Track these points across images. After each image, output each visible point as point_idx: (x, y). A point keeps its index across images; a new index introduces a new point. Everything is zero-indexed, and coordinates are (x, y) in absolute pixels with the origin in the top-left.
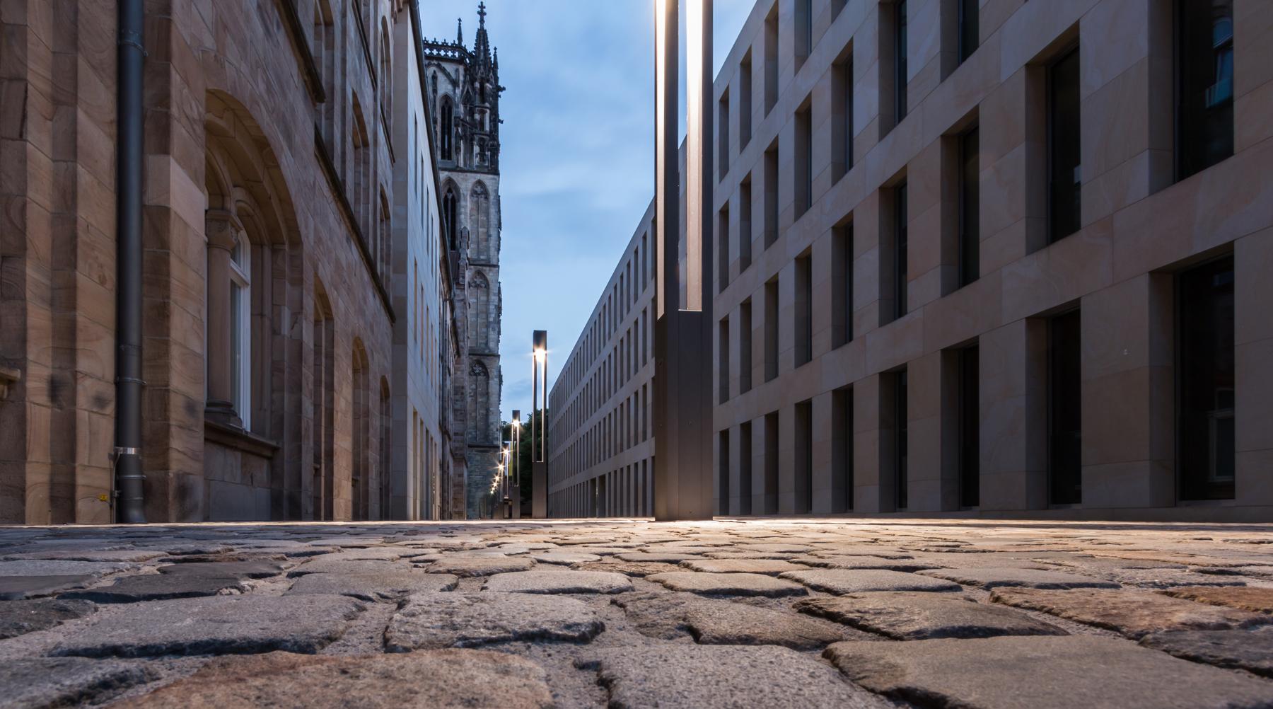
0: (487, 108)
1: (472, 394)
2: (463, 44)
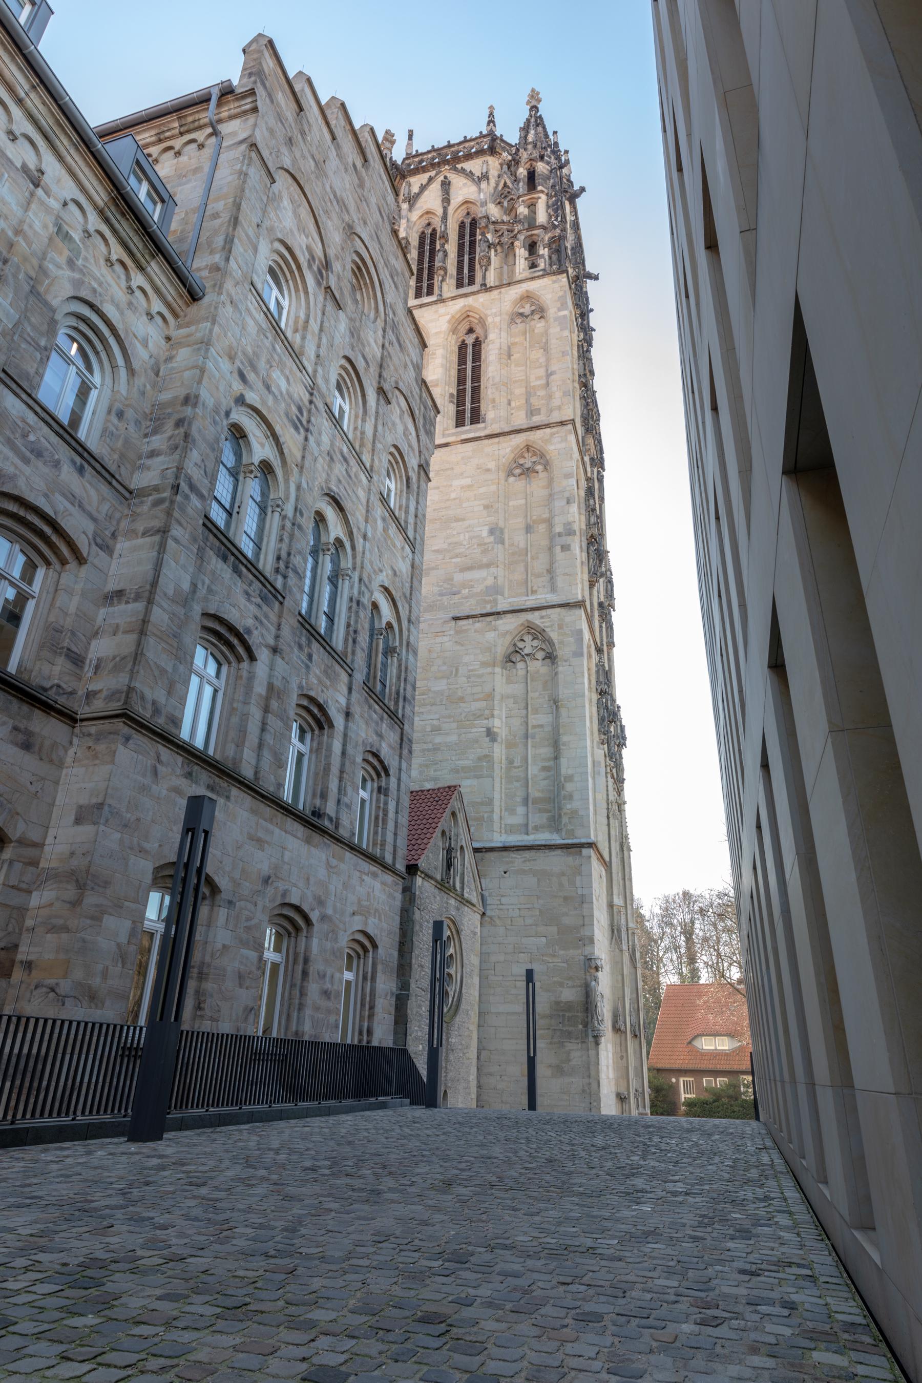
0: (542, 192)
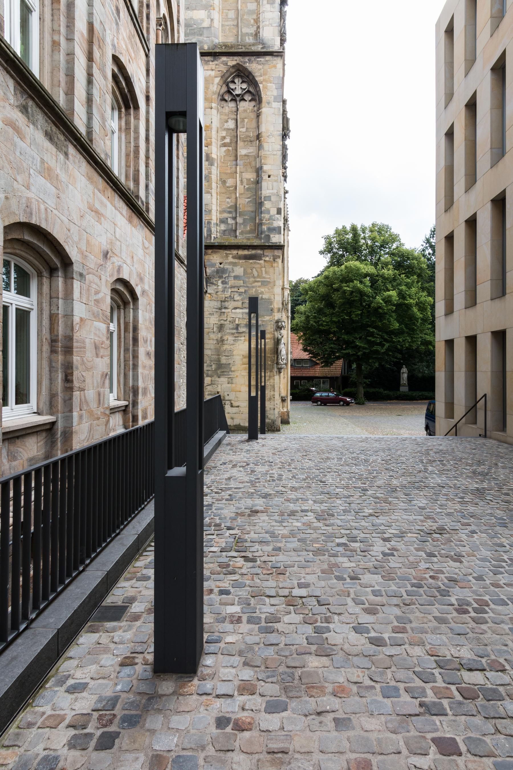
1: (228, 140)
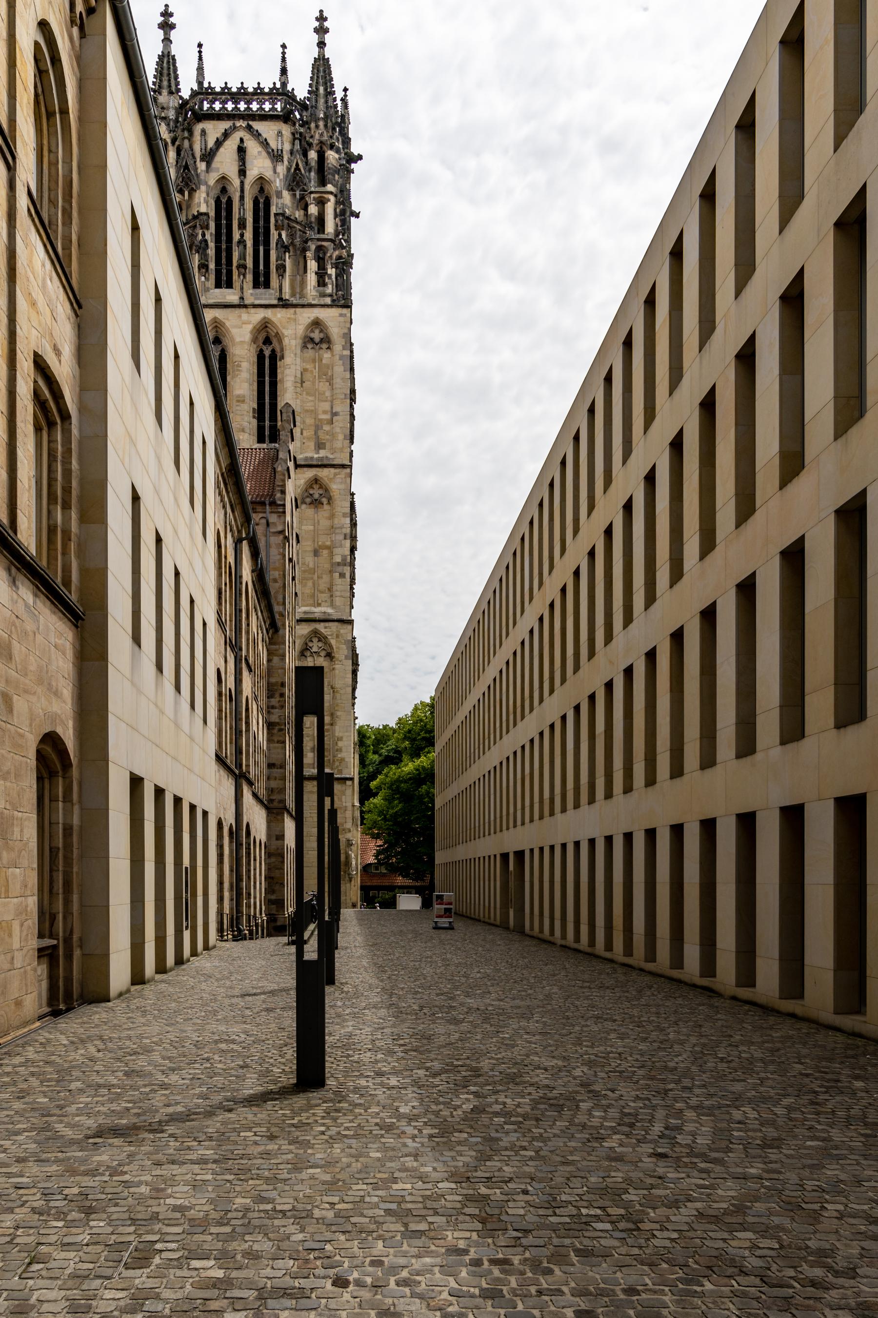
0: (331, 193)
2: (289, 88)
